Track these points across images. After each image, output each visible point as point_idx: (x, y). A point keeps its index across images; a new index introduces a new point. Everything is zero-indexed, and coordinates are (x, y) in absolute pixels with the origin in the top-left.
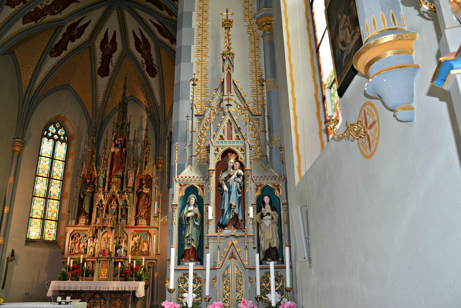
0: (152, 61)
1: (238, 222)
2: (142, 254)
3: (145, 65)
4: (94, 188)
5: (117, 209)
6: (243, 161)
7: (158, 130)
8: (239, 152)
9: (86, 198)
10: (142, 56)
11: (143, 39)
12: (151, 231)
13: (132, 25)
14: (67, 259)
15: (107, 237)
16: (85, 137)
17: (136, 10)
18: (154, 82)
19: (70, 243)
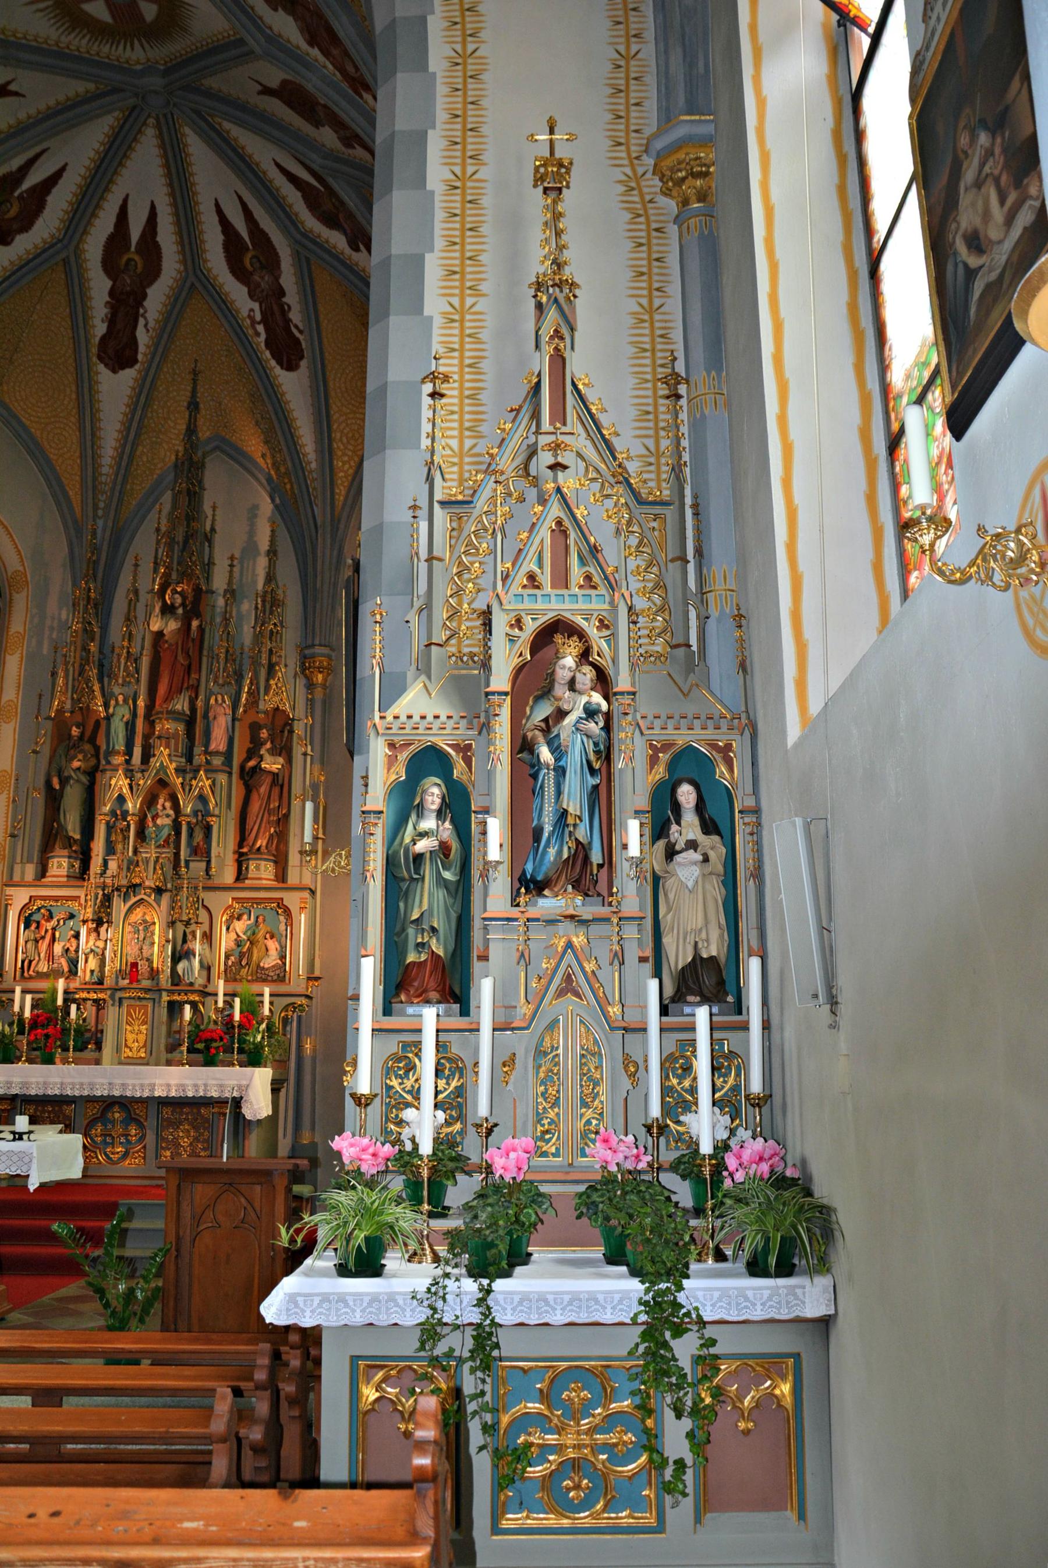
1: (585, 873)
2: (261, 976)
3: (260, 328)
4: (97, 755)
5: (176, 826)
6: (605, 662)
7: (310, 556)
8: (592, 631)
9: (68, 789)
10: (252, 296)
11: (251, 233)
12: (292, 900)
13: (213, 182)
14: (13, 992)
15: (145, 921)
16: (59, 580)
17: (227, 125)
18: (293, 385)
19: (22, 941)
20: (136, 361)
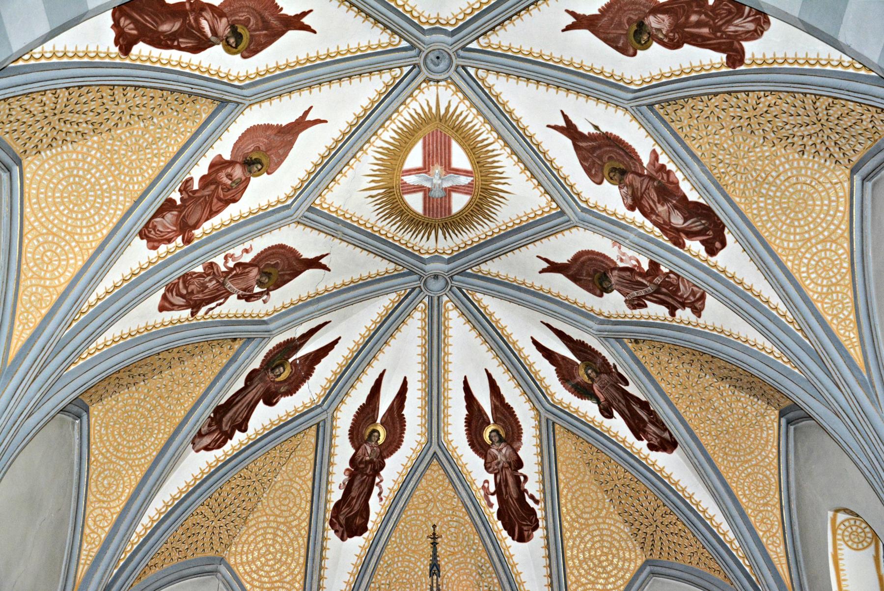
0: (519, 483)
3: (494, 499)
11: (495, 409)
13: (522, 327)
20: (366, 529)
